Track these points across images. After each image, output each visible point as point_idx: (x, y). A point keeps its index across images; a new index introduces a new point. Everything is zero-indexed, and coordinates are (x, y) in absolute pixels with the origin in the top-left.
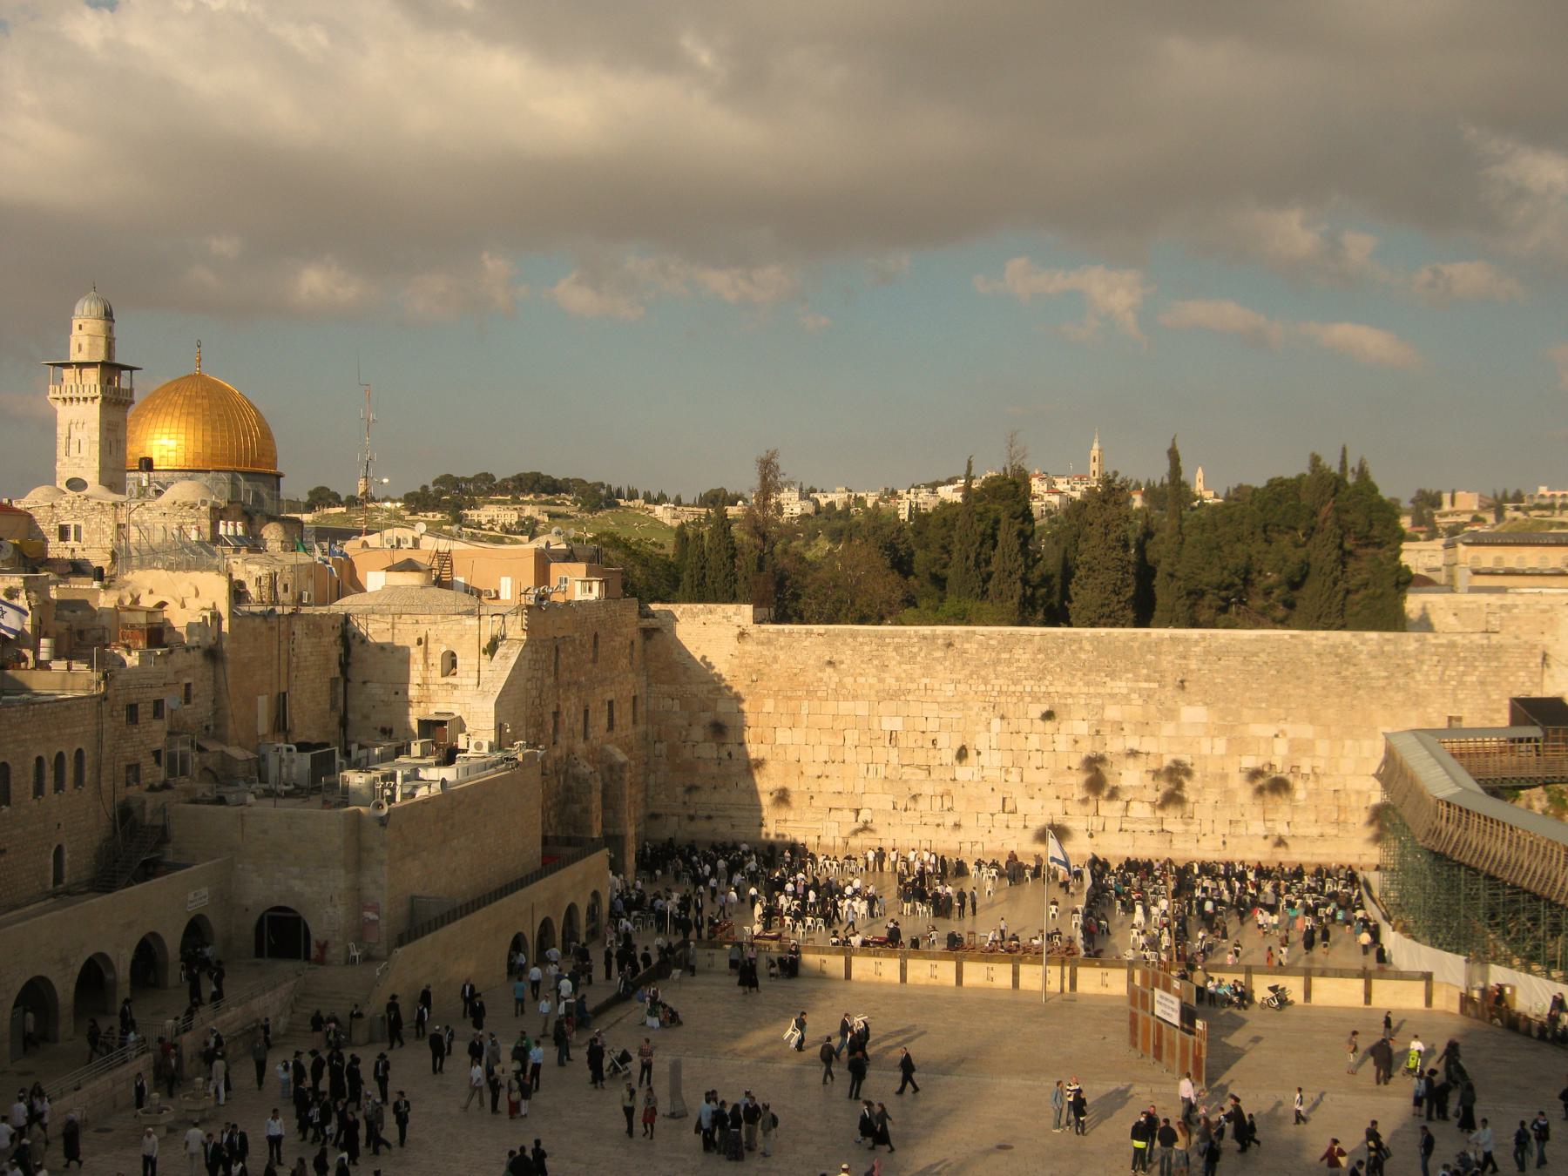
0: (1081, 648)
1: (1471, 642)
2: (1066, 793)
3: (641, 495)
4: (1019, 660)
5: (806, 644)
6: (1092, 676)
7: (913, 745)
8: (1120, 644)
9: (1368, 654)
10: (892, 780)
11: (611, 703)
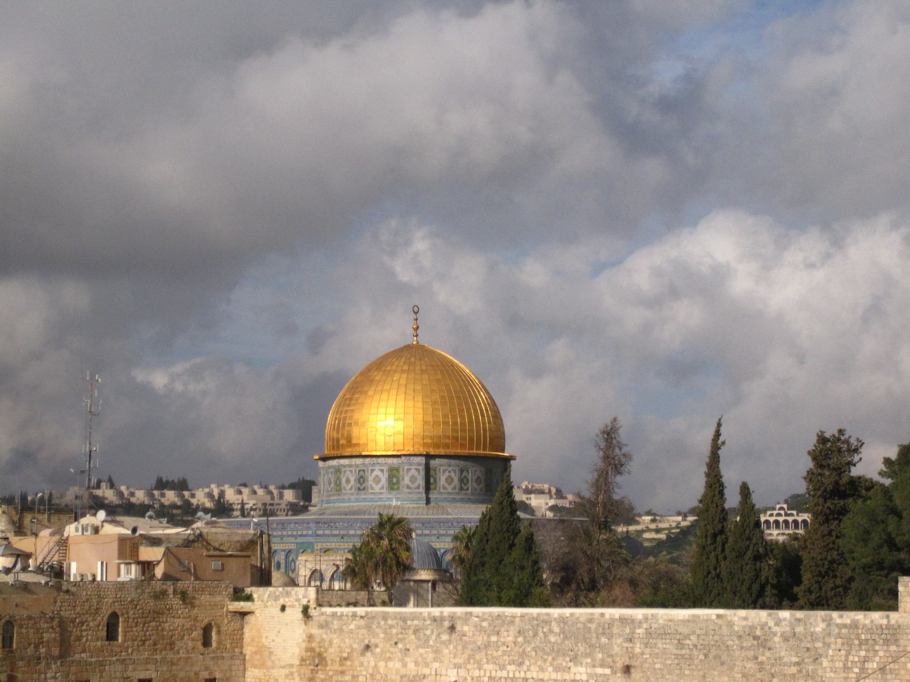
0: (551, 631)
1: (872, 622)
4: (504, 644)
5: (352, 627)
6: (560, 661)
9: (782, 635)
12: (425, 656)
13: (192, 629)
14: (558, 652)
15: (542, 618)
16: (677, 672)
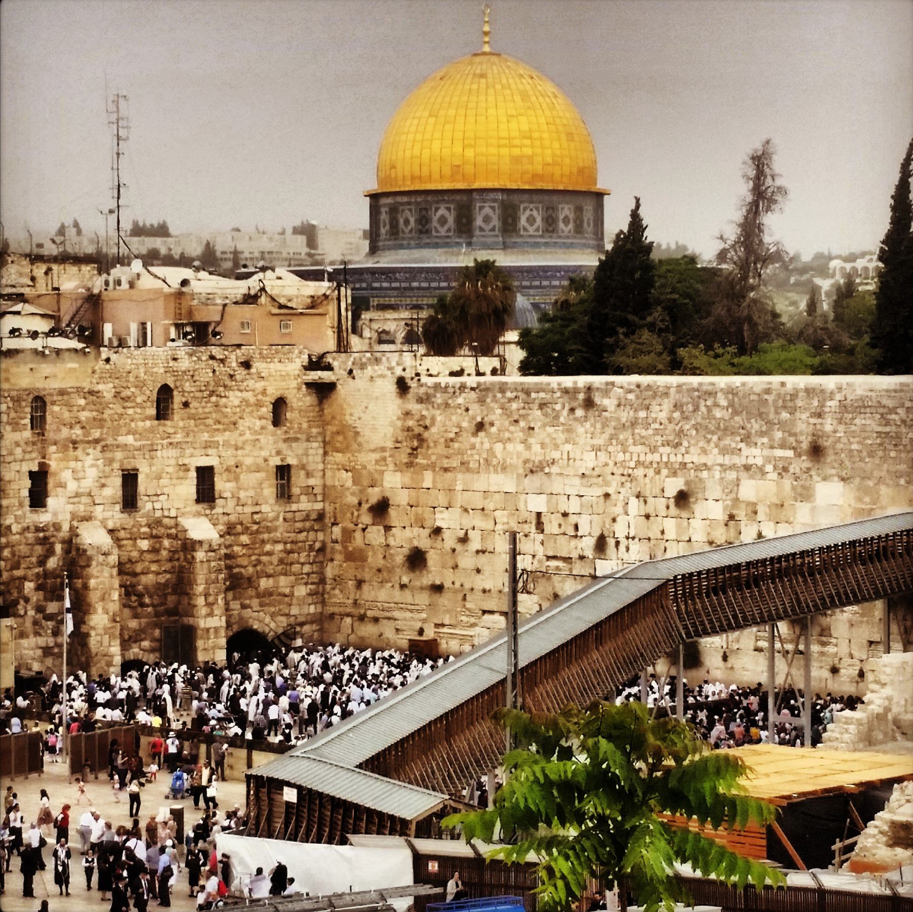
0: (716, 405)
4: (655, 421)
6: (727, 441)
7: (556, 530)
12: (554, 436)
13: (259, 405)
14: (726, 430)
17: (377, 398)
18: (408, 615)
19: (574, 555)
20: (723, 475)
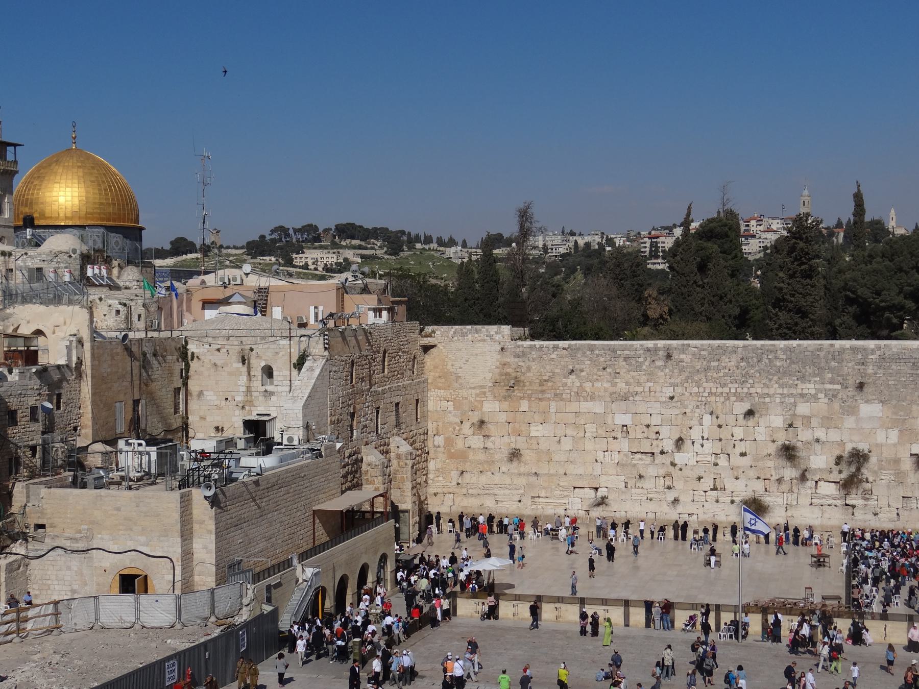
0: (776, 358)
2: (765, 474)
3: (435, 240)
4: (725, 368)
5: (553, 356)
6: (786, 380)
7: (640, 436)
8: (809, 353)
10: (623, 465)
11: (397, 404)
14: (785, 373)
15: (767, 348)
16: (913, 386)
17: (477, 355)
18: (507, 492)
19: (657, 451)
20: (783, 400)
